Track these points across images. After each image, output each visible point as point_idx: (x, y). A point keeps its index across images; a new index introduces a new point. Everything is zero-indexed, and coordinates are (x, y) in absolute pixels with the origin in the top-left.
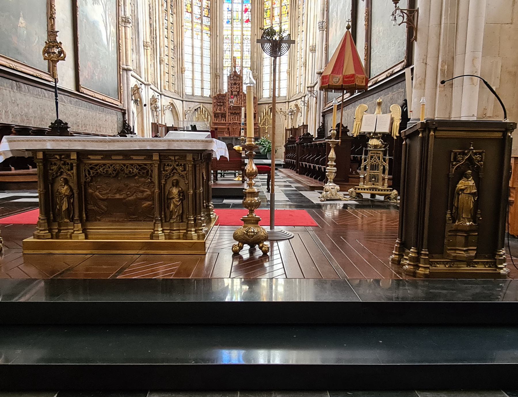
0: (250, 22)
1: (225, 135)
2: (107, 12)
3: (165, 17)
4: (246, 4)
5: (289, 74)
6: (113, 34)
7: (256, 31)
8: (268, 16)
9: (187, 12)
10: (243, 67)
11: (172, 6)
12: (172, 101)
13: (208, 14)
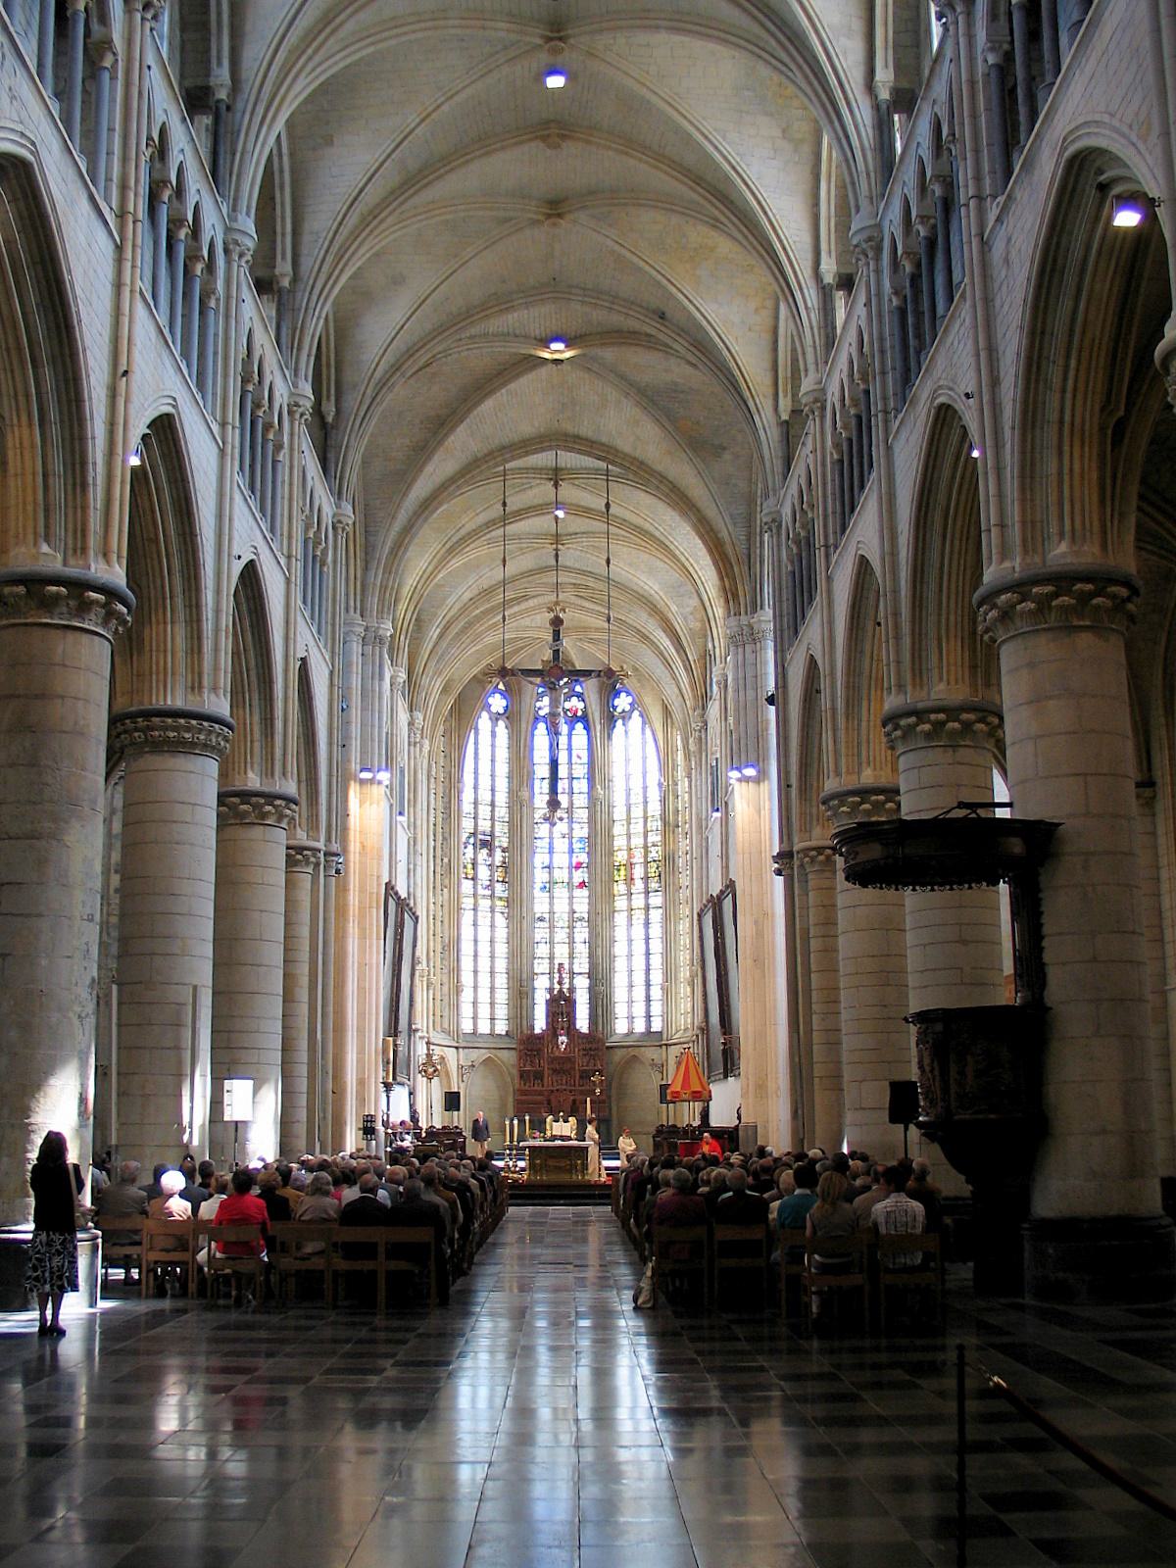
8: (623, 878)
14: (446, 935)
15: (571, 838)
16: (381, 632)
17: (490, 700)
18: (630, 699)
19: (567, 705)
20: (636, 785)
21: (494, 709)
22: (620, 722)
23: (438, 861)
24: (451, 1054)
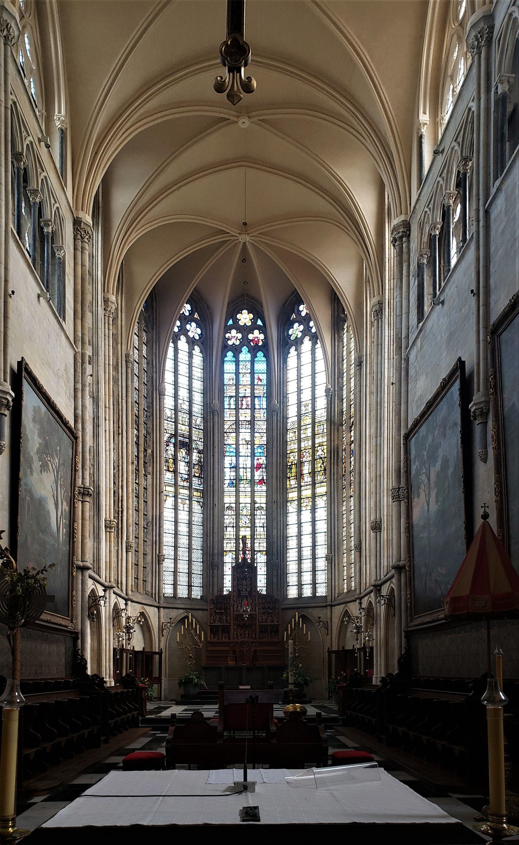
1: (229, 662)
2: (59, 483)
3: (136, 480)
6: (65, 514)
10: (255, 551)
11: (146, 463)
15: (253, 444)
20: (306, 396)
22: (293, 349)
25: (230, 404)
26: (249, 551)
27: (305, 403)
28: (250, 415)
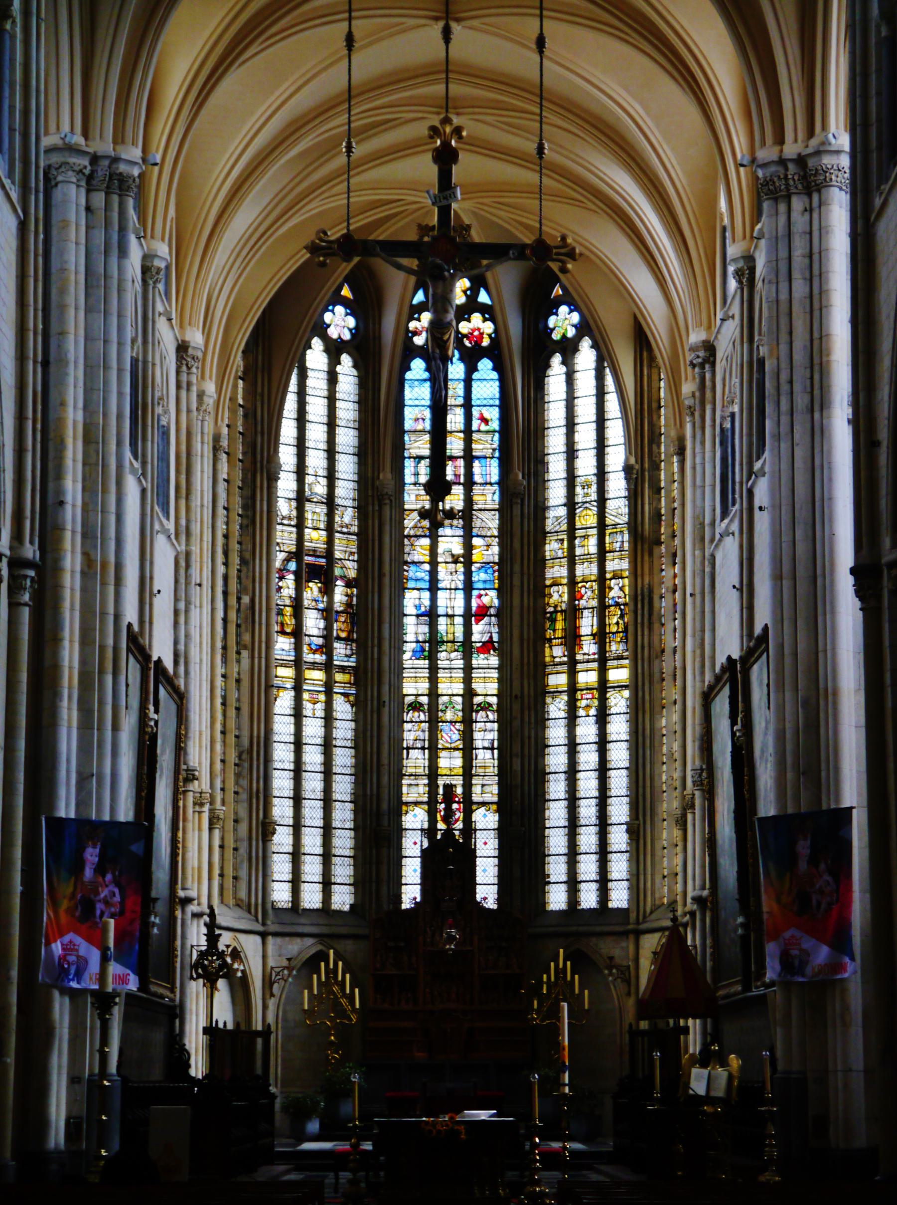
0: (495, 649)
4: (482, 592)
5: (634, 837)
7: (516, 684)
8: (559, 634)
9: (283, 632)
12: (236, 939)
13: (350, 632)
14: (246, 733)
16: (122, 168)
17: (328, 317)
18: (575, 317)
19: (464, 327)
20: (586, 465)
21: (333, 333)
22: (557, 359)
23: (233, 601)
24: (251, 945)
25: (417, 474)
26: (459, 803)
27: (583, 479)
28: (462, 497)
